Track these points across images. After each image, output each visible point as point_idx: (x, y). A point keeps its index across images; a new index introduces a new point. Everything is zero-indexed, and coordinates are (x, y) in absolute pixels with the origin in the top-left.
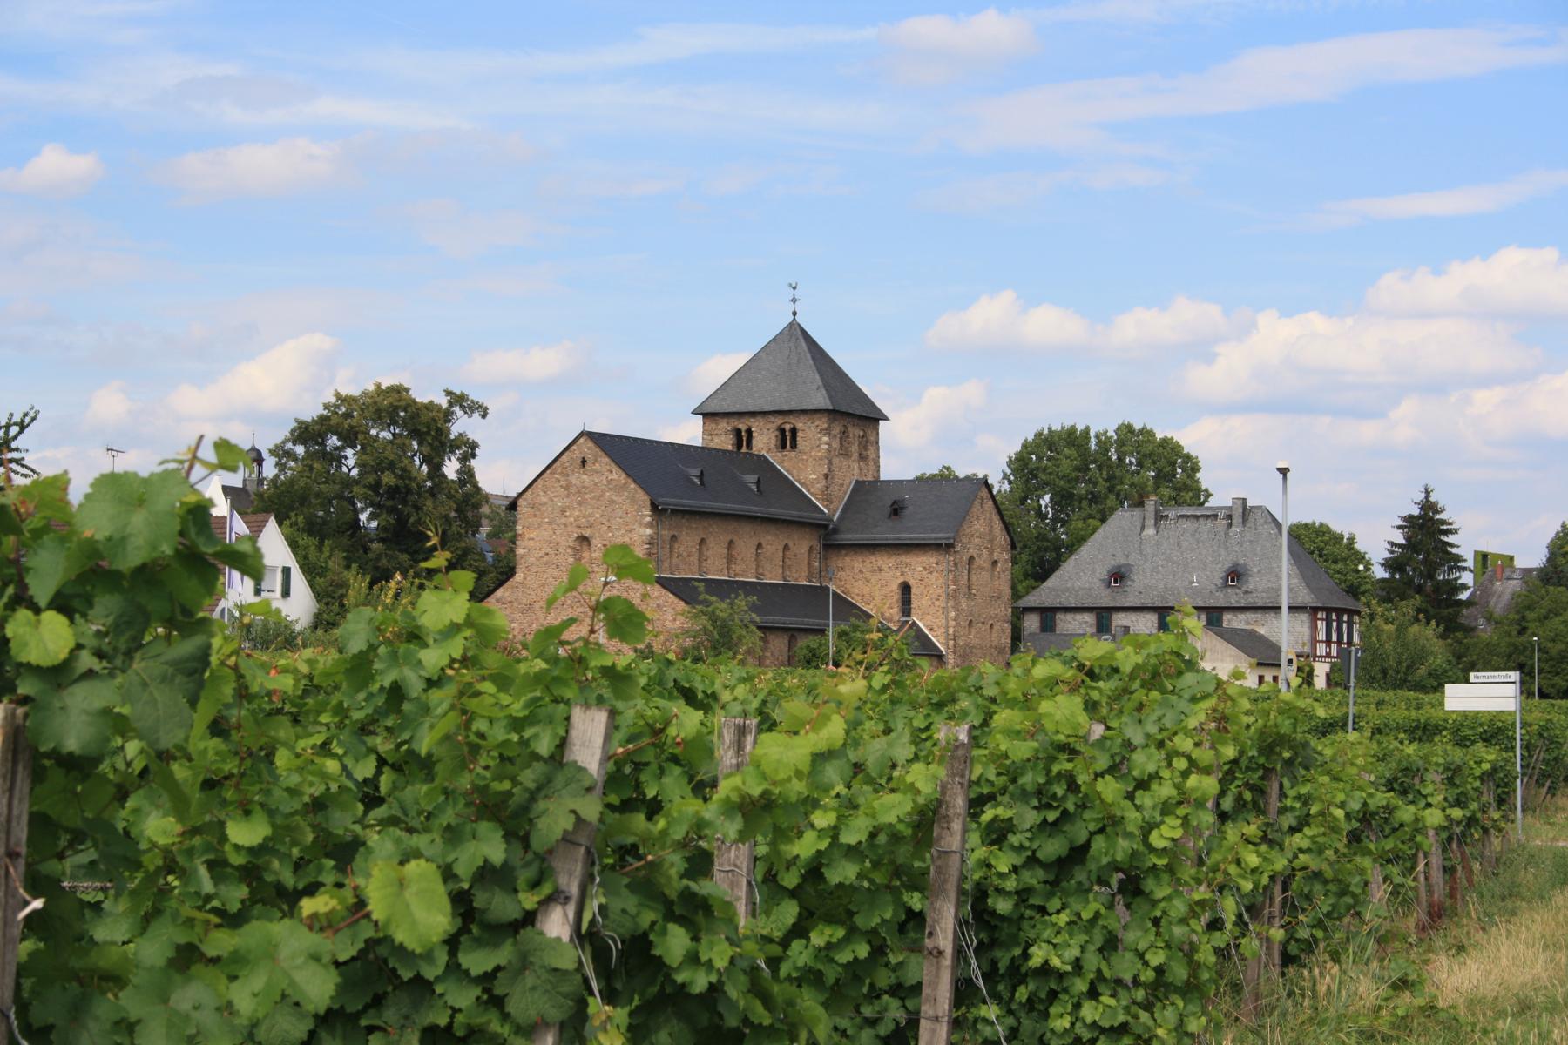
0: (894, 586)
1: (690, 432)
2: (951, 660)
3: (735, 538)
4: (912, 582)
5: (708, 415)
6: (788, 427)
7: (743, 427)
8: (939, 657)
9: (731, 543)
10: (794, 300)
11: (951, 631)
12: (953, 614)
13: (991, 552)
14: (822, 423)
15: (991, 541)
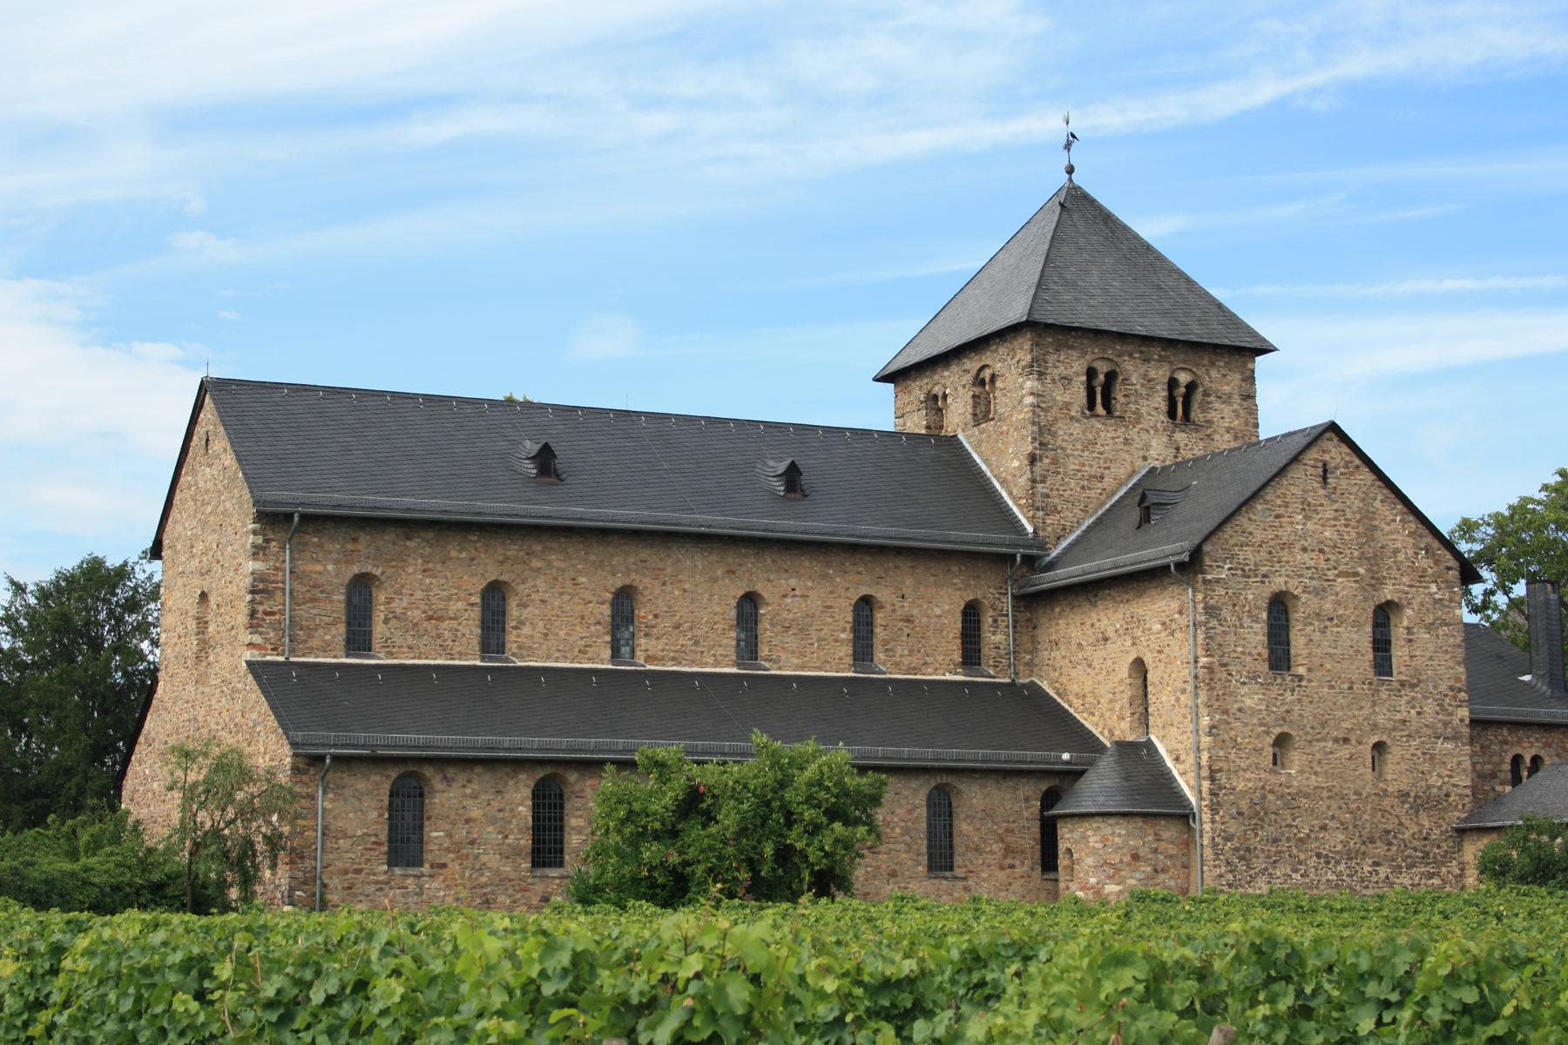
0: (1124, 671)
1: (878, 411)
2: (1206, 825)
3: (643, 582)
4: (1148, 659)
5: (895, 377)
6: (987, 374)
7: (937, 390)
8: (1184, 817)
9: (865, 607)
10: (1068, 146)
11: (1205, 756)
12: (1205, 721)
13: (1377, 582)
14: (1024, 349)
15: (1373, 561)
